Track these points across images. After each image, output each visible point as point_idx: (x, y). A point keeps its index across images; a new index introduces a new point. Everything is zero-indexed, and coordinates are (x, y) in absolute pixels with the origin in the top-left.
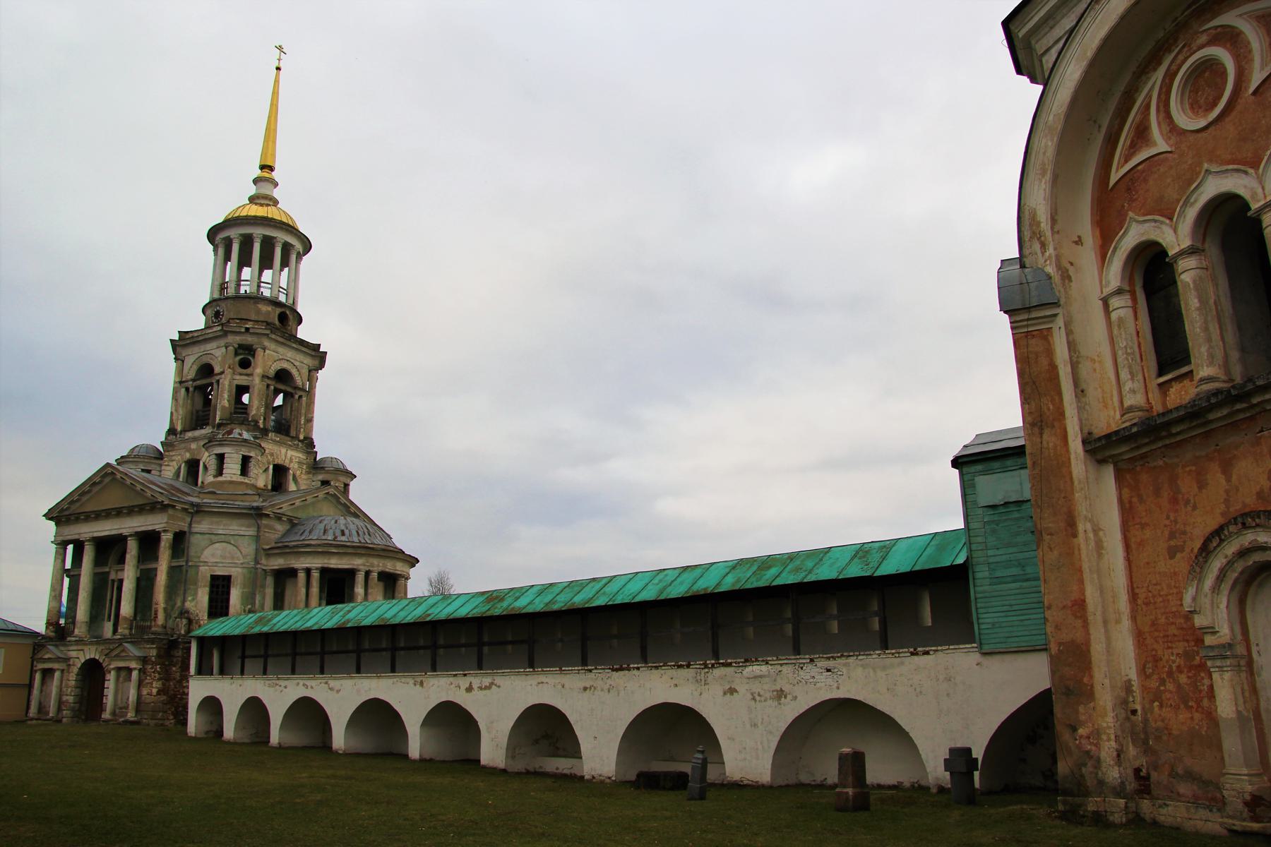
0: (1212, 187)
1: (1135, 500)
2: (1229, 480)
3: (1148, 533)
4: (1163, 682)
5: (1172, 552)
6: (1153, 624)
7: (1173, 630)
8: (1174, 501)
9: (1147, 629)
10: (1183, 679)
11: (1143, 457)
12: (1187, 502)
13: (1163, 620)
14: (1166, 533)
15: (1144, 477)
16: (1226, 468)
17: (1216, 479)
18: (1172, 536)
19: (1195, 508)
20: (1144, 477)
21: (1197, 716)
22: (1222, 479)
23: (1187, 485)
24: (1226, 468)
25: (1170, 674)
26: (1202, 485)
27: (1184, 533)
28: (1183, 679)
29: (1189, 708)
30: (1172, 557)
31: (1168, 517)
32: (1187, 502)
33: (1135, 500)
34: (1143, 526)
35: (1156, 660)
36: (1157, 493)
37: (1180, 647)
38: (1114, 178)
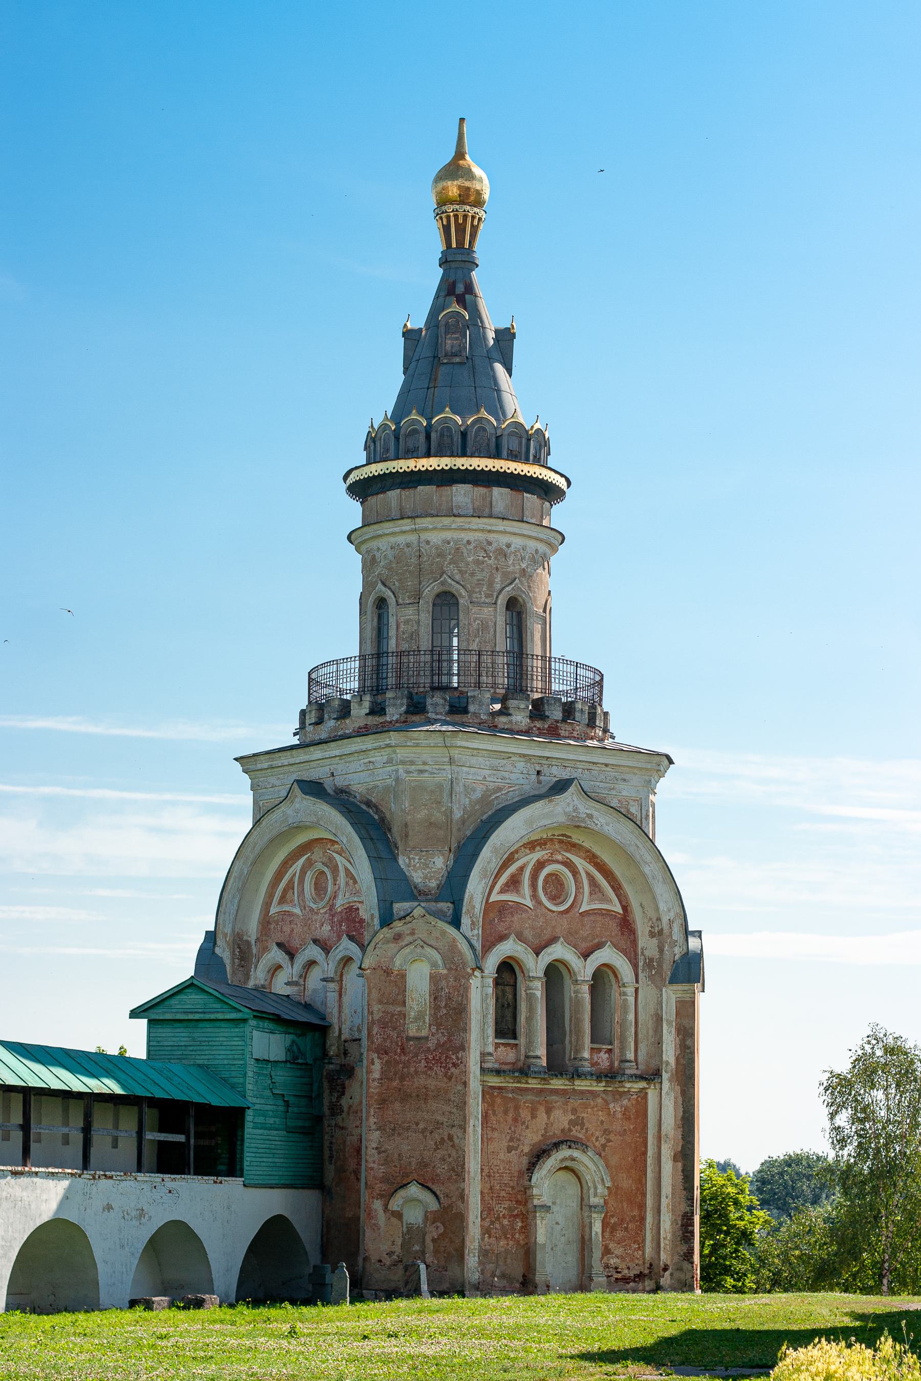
0: (559, 951)
1: (490, 1112)
2: (549, 1118)
3: (496, 1134)
4: (492, 1223)
5: (510, 1149)
6: (491, 1188)
7: (503, 1194)
8: (515, 1120)
9: (486, 1191)
10: (506, 1222)
11: (500, 1088)
12: (524, 1123)
13: (498, 1187)
14: (508, 1137)
15: (499, 1100)
16: (549, 1111)
18: (511, 1140)
19: (527, 1127)
20: (499, 1100)
21: (511, 1243)
22: (545, 1116)
23: (525, 1114)
24: (549, 1111)
25: (498, 1218)
26: (534, 1117)
27: (519, 1140)
28: (506, 1222)
29: (507, 1238)
30: (509, 1152)
31: (510, 1129)
32: (524, 1123)
33: (490, 1112)
34: (493, 1129)
35: (490, 1210)
36: (506, 1112)
37: (507, 1204)
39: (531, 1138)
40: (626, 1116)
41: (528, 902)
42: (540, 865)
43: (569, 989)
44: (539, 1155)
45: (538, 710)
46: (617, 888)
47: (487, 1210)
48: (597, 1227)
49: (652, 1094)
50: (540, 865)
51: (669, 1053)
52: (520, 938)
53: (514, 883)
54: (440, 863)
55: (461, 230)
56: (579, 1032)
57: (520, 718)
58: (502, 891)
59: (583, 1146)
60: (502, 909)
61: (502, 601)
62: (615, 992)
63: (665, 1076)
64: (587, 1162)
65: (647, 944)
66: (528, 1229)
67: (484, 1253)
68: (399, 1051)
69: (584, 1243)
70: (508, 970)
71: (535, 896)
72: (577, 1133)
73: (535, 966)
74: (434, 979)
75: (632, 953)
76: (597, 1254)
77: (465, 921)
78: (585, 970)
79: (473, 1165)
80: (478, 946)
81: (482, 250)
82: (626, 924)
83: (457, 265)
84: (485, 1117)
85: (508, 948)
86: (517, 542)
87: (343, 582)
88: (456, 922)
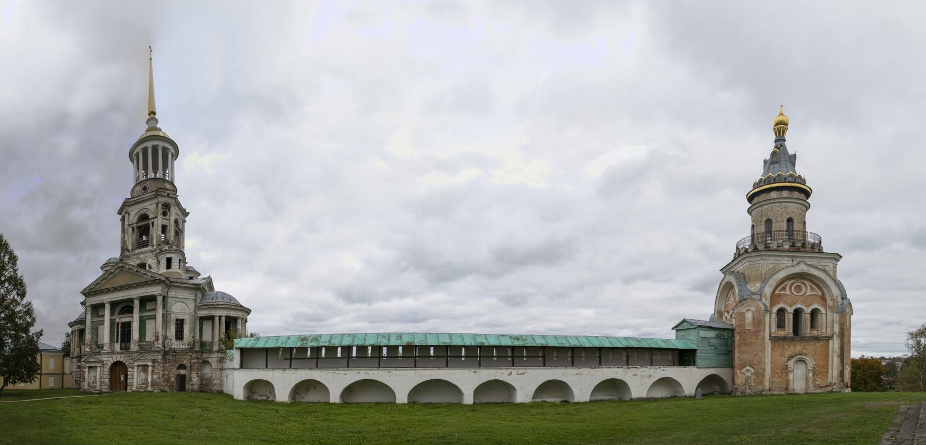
0: (799, 306)
17: (792, 348)
23: (786, 347)
38: (777, 292)
39: (788, 353)
40: (822, 346)
41: (788, 292)
42: (793, 284)
43: (803, 316)
44: (791, 357)
45: (793, 246)
46: (820, 289)
47: (773, 371)
48: (811, 374)
49: (831, 342)
50: (793, 284)
51: (837, 329)
52: (785, 303)
53: (784, 289)
54: (758, 285)
55: (779, 131)
56: (806, 326)
57: (787, 247)
58: (781, 290)
59: (806, 355)
60: (779, 295)
61: (785, 220)
62: (819, 316)
63: (835, 338)
64: (809, 359)
65: (829, 302)
66: (787, 375)
67: (771, 382)
68: (744, 332)
69: (807, 379)
70: (781, 311)
71: (791, 291)
72: (804, 351)
73: (790, 310)
74: (753, 314)
75: (825, 306)
76: (811, 381)
77: (764, 300)
78: (808, 310)
79: (768, 361)
80: (768, 305)
81: (787, 136)
82: (823, 298)
83: (780, 140)
84: (772, 349)
85: (781, 305)
86: (790, 204)
87: (748, 220)
88: (760, 300)
